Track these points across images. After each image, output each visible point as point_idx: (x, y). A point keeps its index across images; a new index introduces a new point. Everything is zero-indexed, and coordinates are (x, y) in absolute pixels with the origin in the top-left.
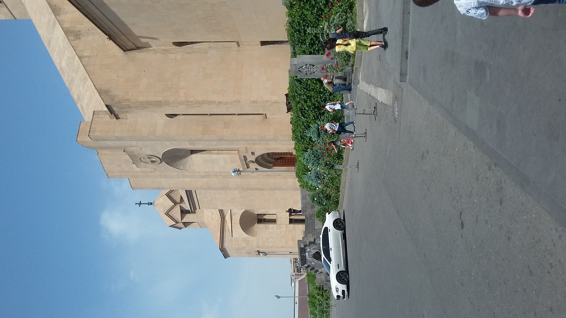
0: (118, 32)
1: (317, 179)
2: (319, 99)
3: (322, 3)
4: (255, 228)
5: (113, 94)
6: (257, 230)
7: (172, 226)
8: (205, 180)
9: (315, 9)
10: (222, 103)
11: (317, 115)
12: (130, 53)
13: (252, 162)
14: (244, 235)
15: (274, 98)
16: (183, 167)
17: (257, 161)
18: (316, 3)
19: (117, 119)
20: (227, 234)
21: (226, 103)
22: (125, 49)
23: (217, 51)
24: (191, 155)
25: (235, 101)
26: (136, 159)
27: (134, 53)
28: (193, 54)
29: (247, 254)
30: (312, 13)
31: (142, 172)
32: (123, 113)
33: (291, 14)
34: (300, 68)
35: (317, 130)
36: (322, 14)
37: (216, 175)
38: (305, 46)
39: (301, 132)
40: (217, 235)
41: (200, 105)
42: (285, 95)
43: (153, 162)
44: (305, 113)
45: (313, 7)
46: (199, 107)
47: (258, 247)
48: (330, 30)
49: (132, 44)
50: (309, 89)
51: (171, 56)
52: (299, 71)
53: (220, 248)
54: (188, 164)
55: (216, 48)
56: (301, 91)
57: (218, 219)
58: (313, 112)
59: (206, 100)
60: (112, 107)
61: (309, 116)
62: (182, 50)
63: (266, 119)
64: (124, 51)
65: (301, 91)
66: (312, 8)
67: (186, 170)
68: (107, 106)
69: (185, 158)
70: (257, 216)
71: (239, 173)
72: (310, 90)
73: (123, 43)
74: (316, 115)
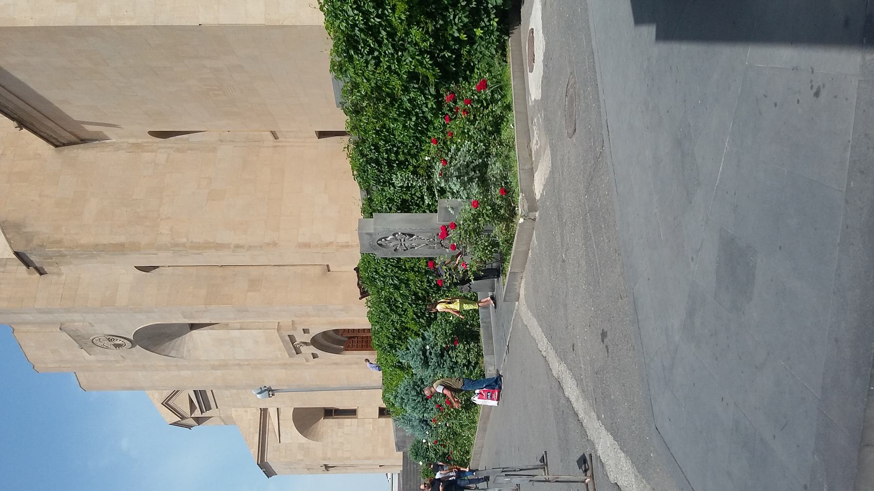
0: (35, 113)
1: (422, 425)
2: (425, 285)
3: (427, 107)
5: (30, 230)
6: (324, 428)
7: (175, 424)
8: (219, 373)
9: (411, 120)
10: (242, 247)
11: (421, 312)
12: (67, 151)
13: (306, 344)
15: (343, 238)
16: (176, 352)
17: (315, 342)
18: (414, 105)
19: (41, 274)
20: (271, 438)
21: (250, 248)
22: (58, 144)
23: (234, 147)
24: (190, 332)
25: (268, 244)
26: (84, 341)
27: (75, 151)
28: (189, 152)
29: (307, 470)
30: (404, 126)
31: (99, 361)
32: (50, 265)
33: (358, 127)
34: (381, 240)
35: (421, 353)
36: (428, 130)
37: (239, 365)
38: (392, 188)
39: (389, 338)
40: (253, 440)
41: (199, 252)
42: (355, 269)
44: (397, 307)
45: (408, 114)
46: (199, 254)
47: (324, 459)
48: (446, 181)
49: (68, 134)
50: (403, 267)
51: (147, 156)
52: (379, 244)
53: (259, 463)
54: (186, 349)
55: (232, 141)
56: (386, 270)
58: (414, 306)
59: (212, 241)
60: (28, 255)
61: (405, 312)
62: (168, 145)
63: (329, 273)
64: (56, 146)
65: (386, 270)
66: (404, 117)
67: (182, 357)
68: (16, 254)
69: (181, 338)
71: (271, 393)
72: (405, 270)
73: (51, 134)
74: (421, 310)
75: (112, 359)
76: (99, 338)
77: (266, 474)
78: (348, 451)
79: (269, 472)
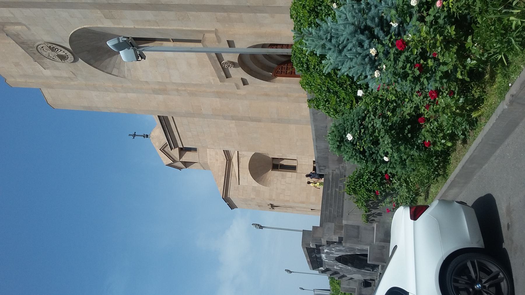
4: (268, 176)
6: (271, 178)
8: (161, 97)
13: (234, 64)
14: (255, 184)
20: (233, 181)
31: (56, 77)
37: (177, 90)
40: (221, 181)
43: (63, 58)
47: (270, 200)
53: (224, 197)
54: (126, 68)
57: (223, 160)
67: (124, 77)
70: (272, 161)
75: (65, 75)
76: (42, 46)
77: (230, 207)
78: (289, 196)
79: (232, 206)
